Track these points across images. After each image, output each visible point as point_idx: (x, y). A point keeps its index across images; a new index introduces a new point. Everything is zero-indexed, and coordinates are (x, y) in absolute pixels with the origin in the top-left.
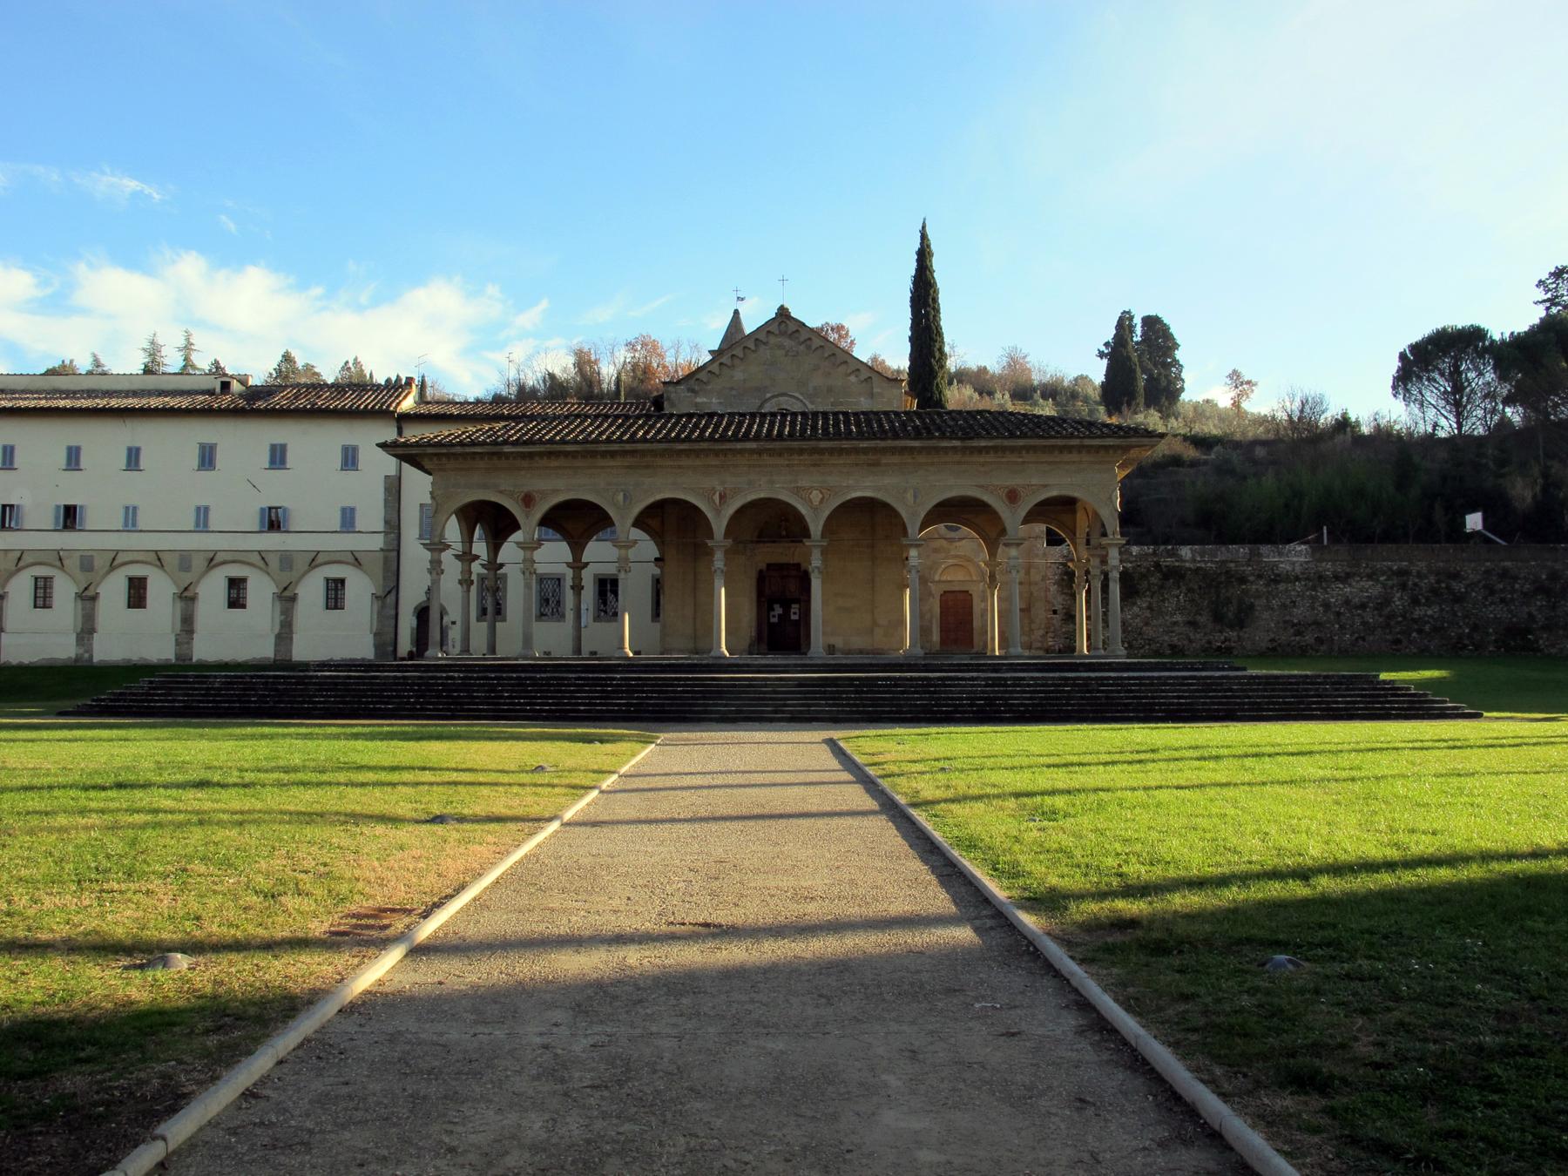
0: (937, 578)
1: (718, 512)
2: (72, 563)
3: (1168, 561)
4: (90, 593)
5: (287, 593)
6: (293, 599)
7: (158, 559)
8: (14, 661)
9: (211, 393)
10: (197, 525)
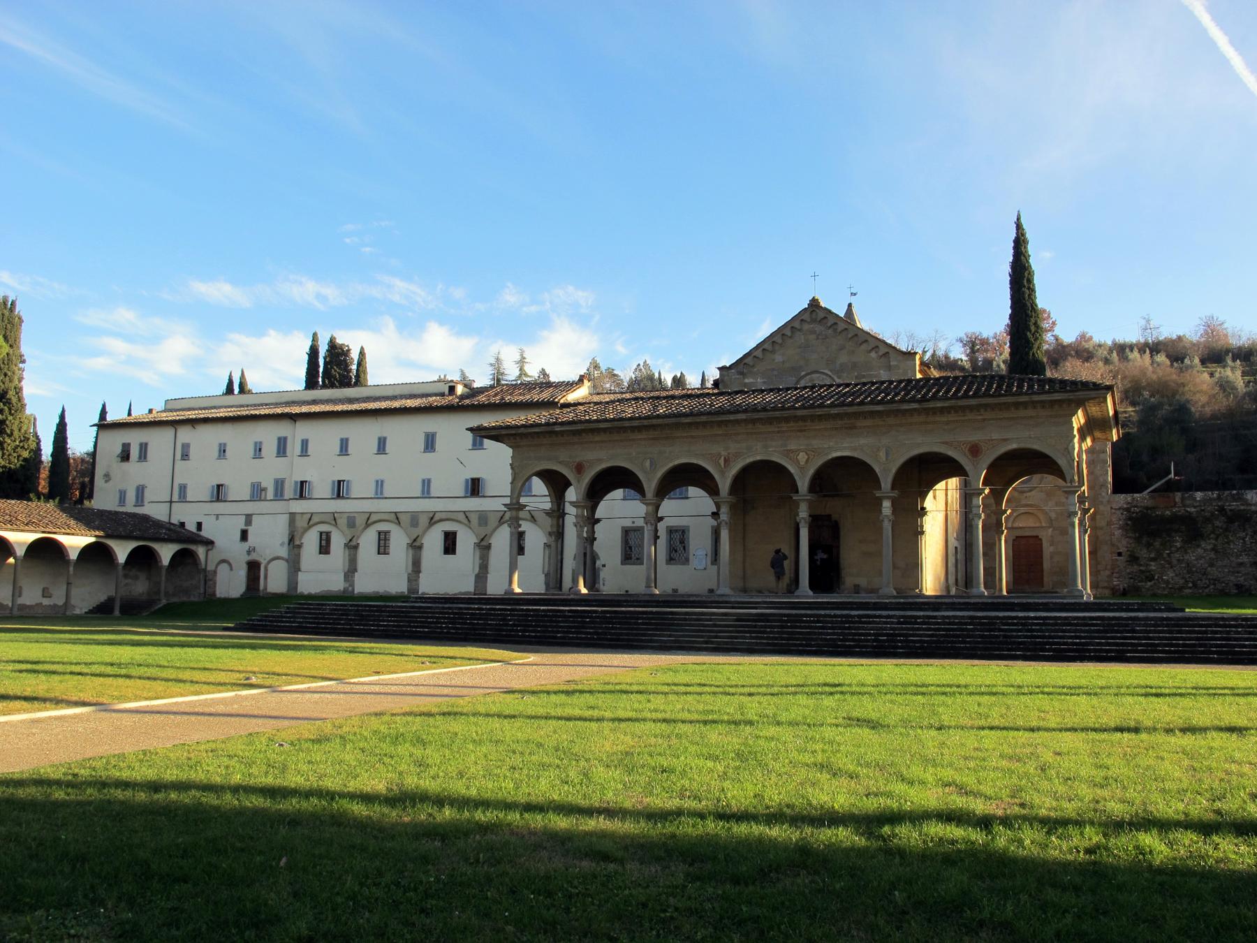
1: (722, 473)
2: (342, 522)
3: (1235, 505)
4: (353, 543)
5: (484, 543)
6: (489, 547)
7: (396, 518)
8: (306, 593)
9: (442, 395)
10: (423, 492)
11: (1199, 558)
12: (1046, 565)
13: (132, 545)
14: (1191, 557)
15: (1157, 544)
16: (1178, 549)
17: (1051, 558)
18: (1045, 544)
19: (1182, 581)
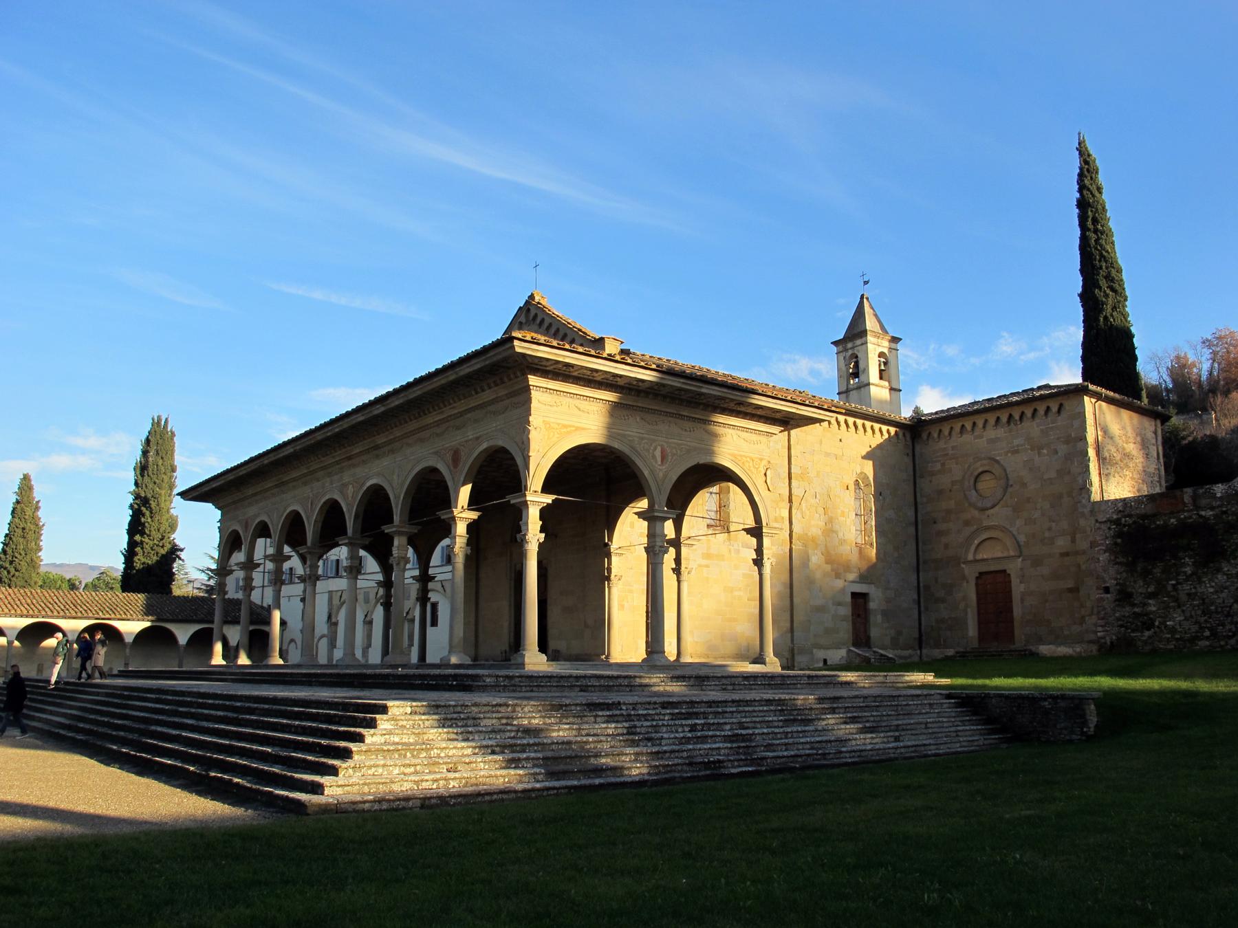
0: (970, 557)
11: (1221, 588)
12: (1017, 611)
13: (193, 628)
14: (1208, 588)
17: (1022, 601)
18: (1015, 581)
19: (1194, 628)
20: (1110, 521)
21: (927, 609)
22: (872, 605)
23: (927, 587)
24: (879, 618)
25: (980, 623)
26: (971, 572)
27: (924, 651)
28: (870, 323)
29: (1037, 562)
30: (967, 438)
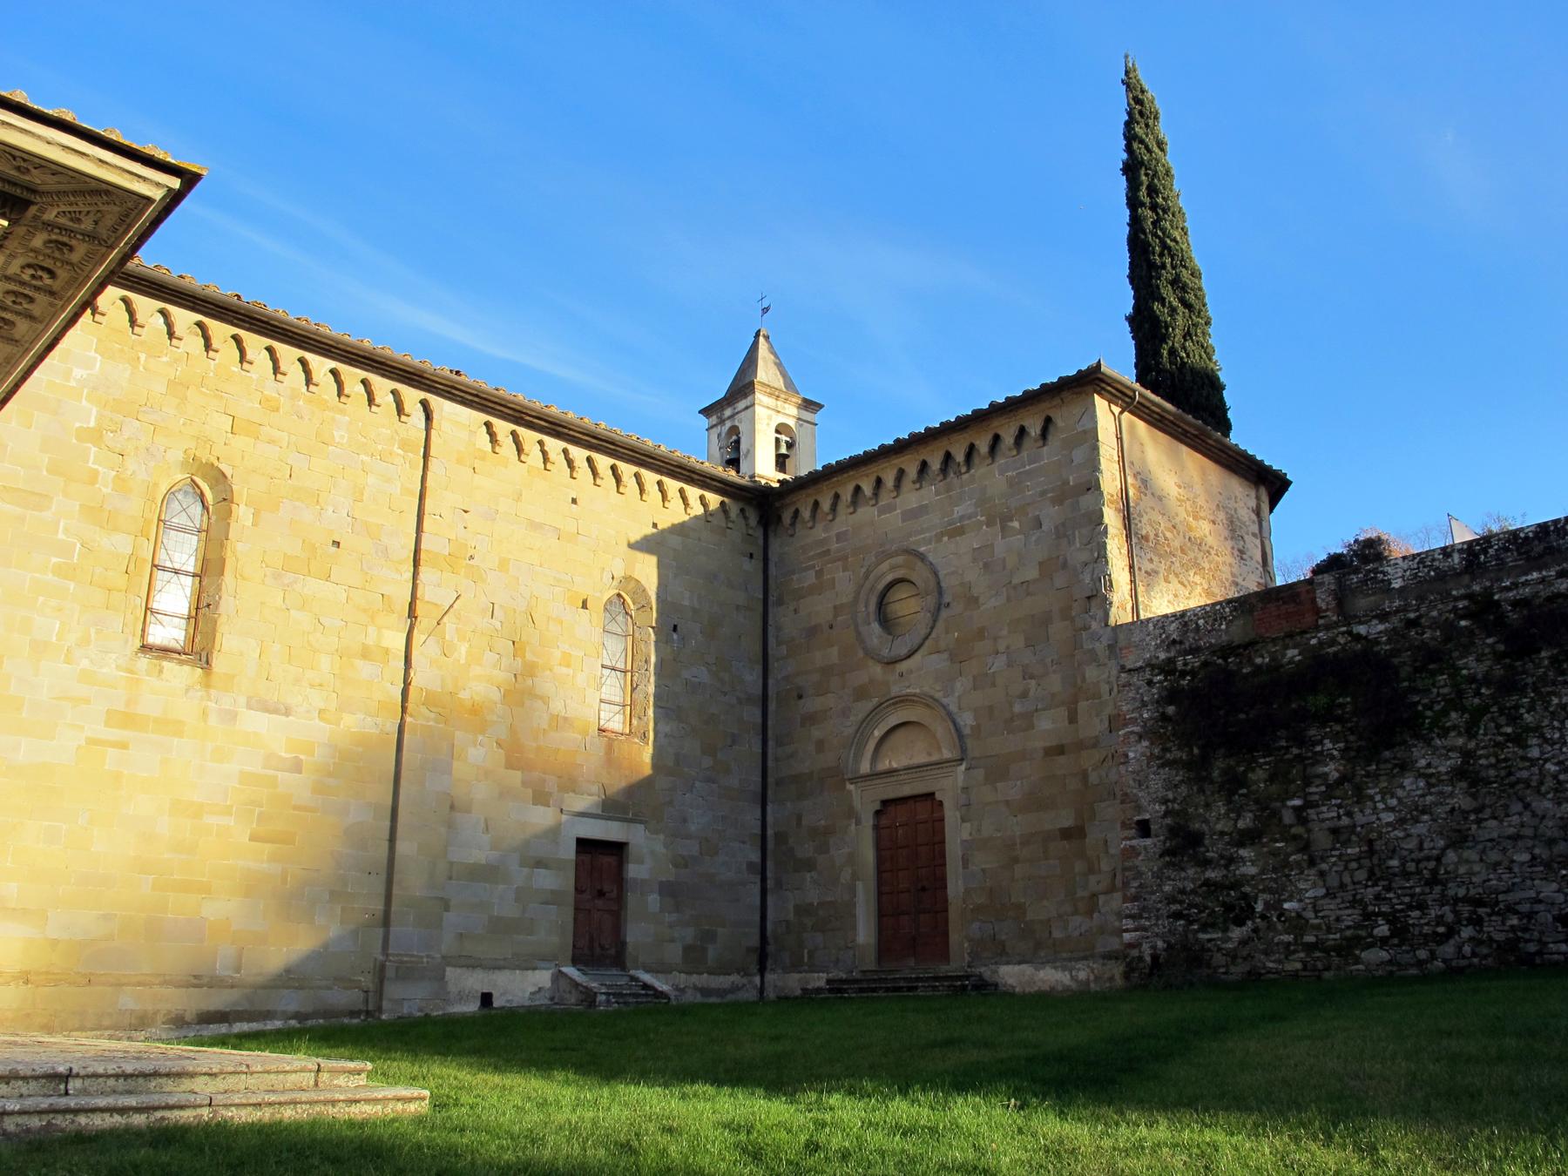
0: (865, 768)
12: (955, 887)
15: (1258, 776)
16: (1331, 789)
17: (966, 862)
18: (951, 815)
19: (1351, 917)
20: (1151, 665)
21: (779, 884)
22: (634, 871)
23: (781, 837)
24: (653, 900)
25: (881, 914)
26: (864, 800)
27: (769, 977)
28: (766, 372)
29: (997, 771)
30: (866, 512)
